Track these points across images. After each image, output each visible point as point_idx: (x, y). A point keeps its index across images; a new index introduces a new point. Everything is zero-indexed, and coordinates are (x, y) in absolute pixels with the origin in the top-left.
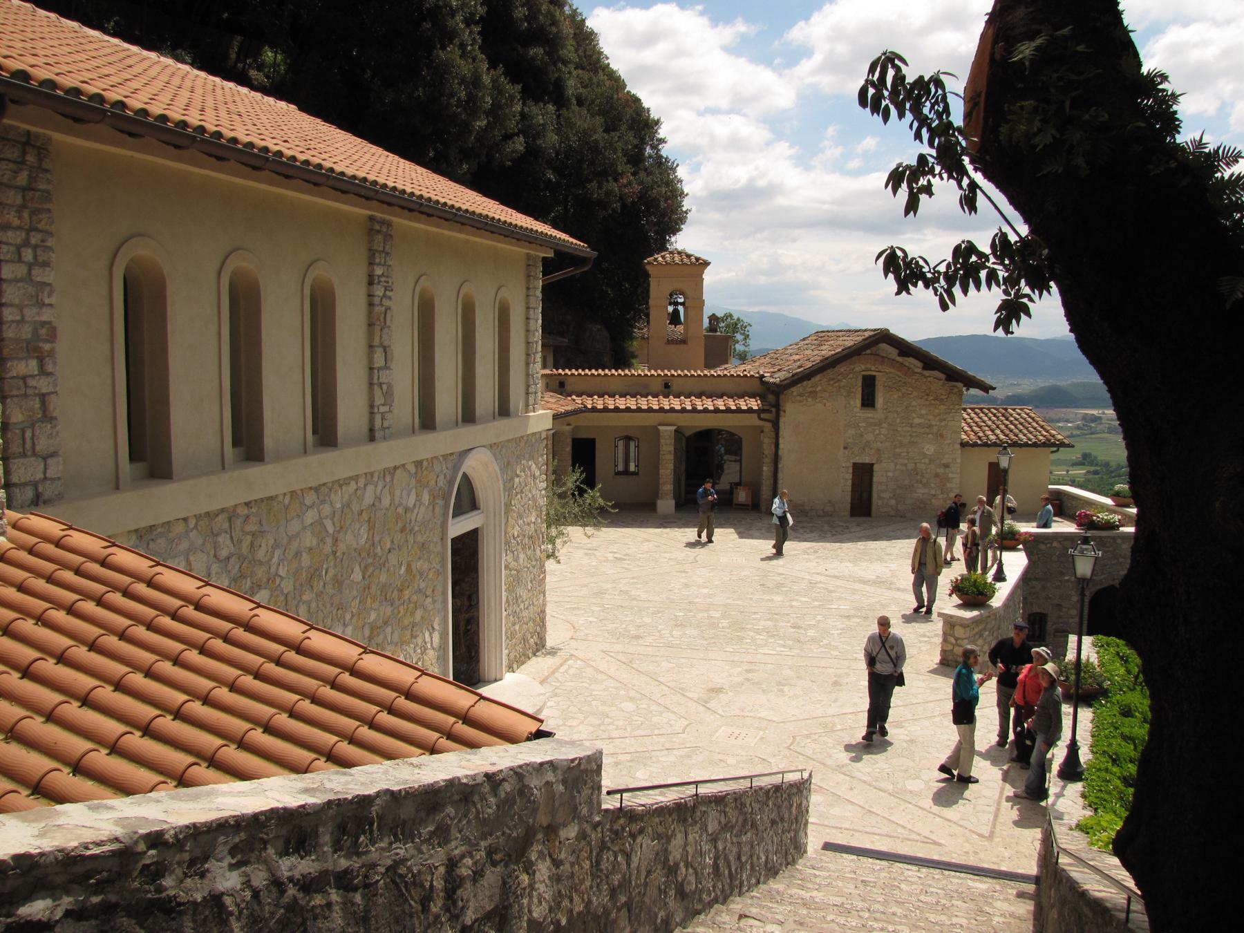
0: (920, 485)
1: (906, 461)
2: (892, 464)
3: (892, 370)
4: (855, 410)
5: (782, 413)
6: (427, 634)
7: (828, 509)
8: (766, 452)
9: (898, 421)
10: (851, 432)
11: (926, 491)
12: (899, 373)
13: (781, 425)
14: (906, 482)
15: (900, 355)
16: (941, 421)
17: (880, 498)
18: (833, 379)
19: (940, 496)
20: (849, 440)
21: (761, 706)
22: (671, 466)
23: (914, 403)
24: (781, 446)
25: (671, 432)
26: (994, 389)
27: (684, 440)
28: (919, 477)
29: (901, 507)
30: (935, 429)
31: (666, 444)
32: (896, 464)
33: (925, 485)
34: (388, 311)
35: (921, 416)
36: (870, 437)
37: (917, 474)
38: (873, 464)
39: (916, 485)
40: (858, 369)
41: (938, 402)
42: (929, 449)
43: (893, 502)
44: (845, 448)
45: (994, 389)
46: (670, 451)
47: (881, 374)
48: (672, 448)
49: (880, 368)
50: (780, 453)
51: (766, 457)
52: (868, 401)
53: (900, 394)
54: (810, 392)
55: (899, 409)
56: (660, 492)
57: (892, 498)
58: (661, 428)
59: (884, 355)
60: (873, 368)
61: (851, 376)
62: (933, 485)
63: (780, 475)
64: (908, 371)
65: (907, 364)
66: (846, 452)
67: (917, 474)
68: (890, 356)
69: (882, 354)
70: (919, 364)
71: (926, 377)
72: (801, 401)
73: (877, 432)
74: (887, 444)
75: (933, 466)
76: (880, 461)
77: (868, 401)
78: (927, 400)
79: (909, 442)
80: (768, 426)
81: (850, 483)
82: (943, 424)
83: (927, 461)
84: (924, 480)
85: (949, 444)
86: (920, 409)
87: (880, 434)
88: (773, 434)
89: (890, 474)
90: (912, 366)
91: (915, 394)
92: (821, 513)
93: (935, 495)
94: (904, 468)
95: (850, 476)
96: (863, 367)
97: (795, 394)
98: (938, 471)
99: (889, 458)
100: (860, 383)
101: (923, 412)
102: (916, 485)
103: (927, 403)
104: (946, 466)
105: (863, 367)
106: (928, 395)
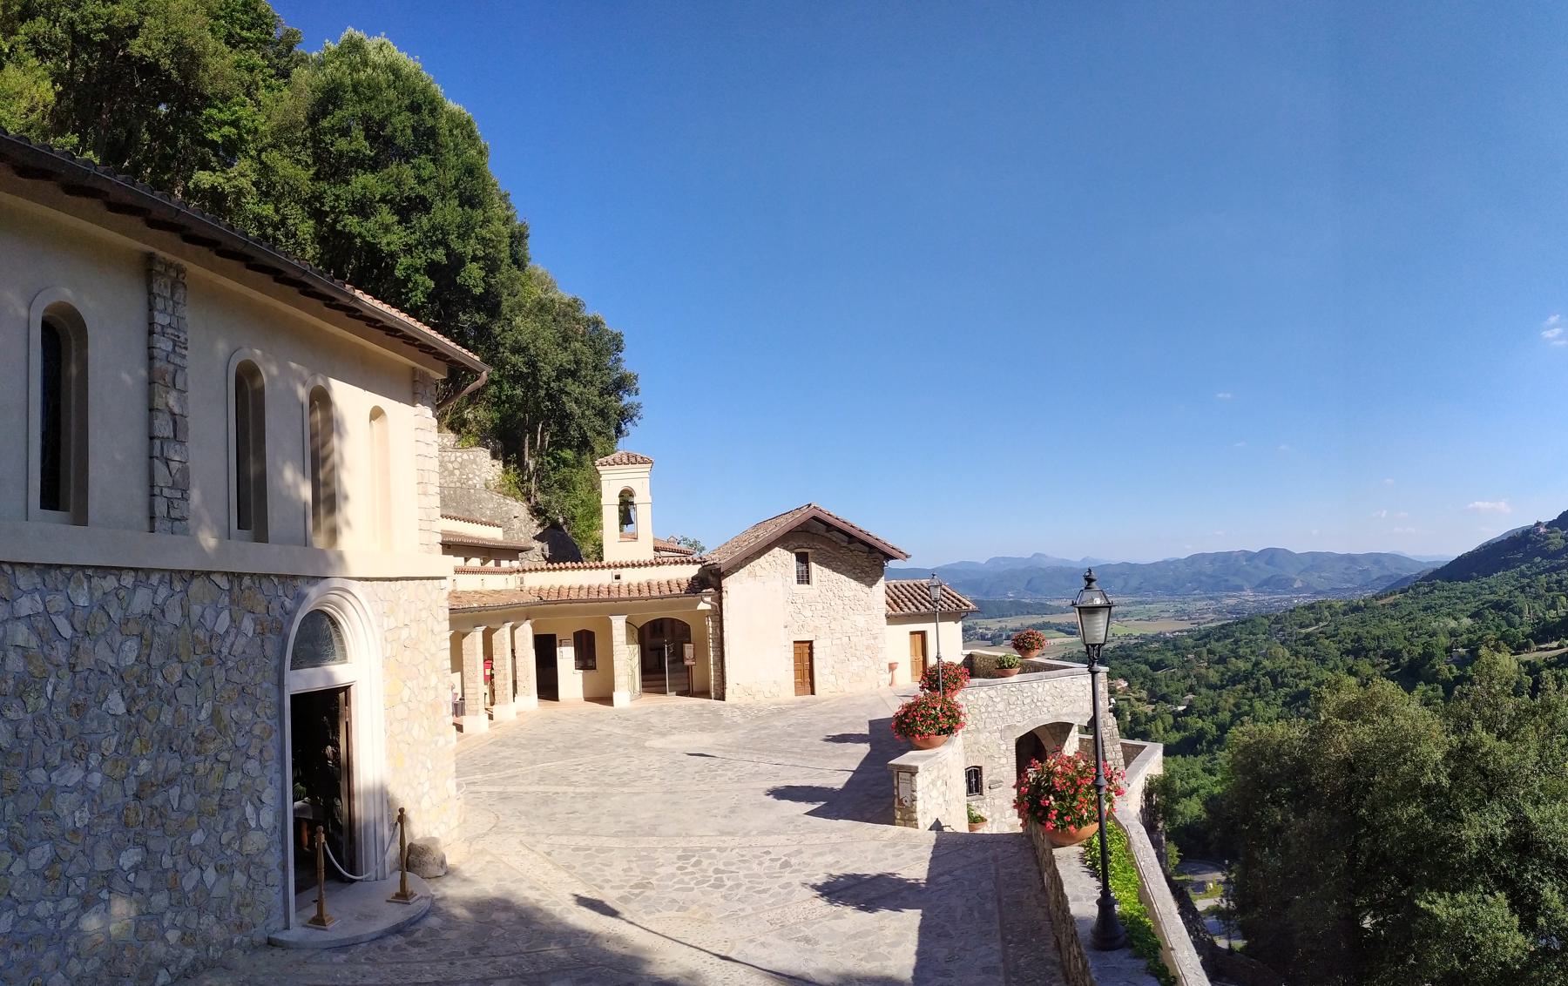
0: (855, 659)
5: (724, 594)
6: (249, 809)
10: (791, 608)
11: (860, 663)
19: (873, 667)
21: (693, 902)
28: (853, 650)
34: (179, 372)
37: (851, 647)
38: (811, 642)
39: (850, 658)
42: (861, 621)
43: (832, 678)
44: (786, 627)
50: (725, 635)
73: (813, 608)
83: (859, 633)
94: (838, 642)
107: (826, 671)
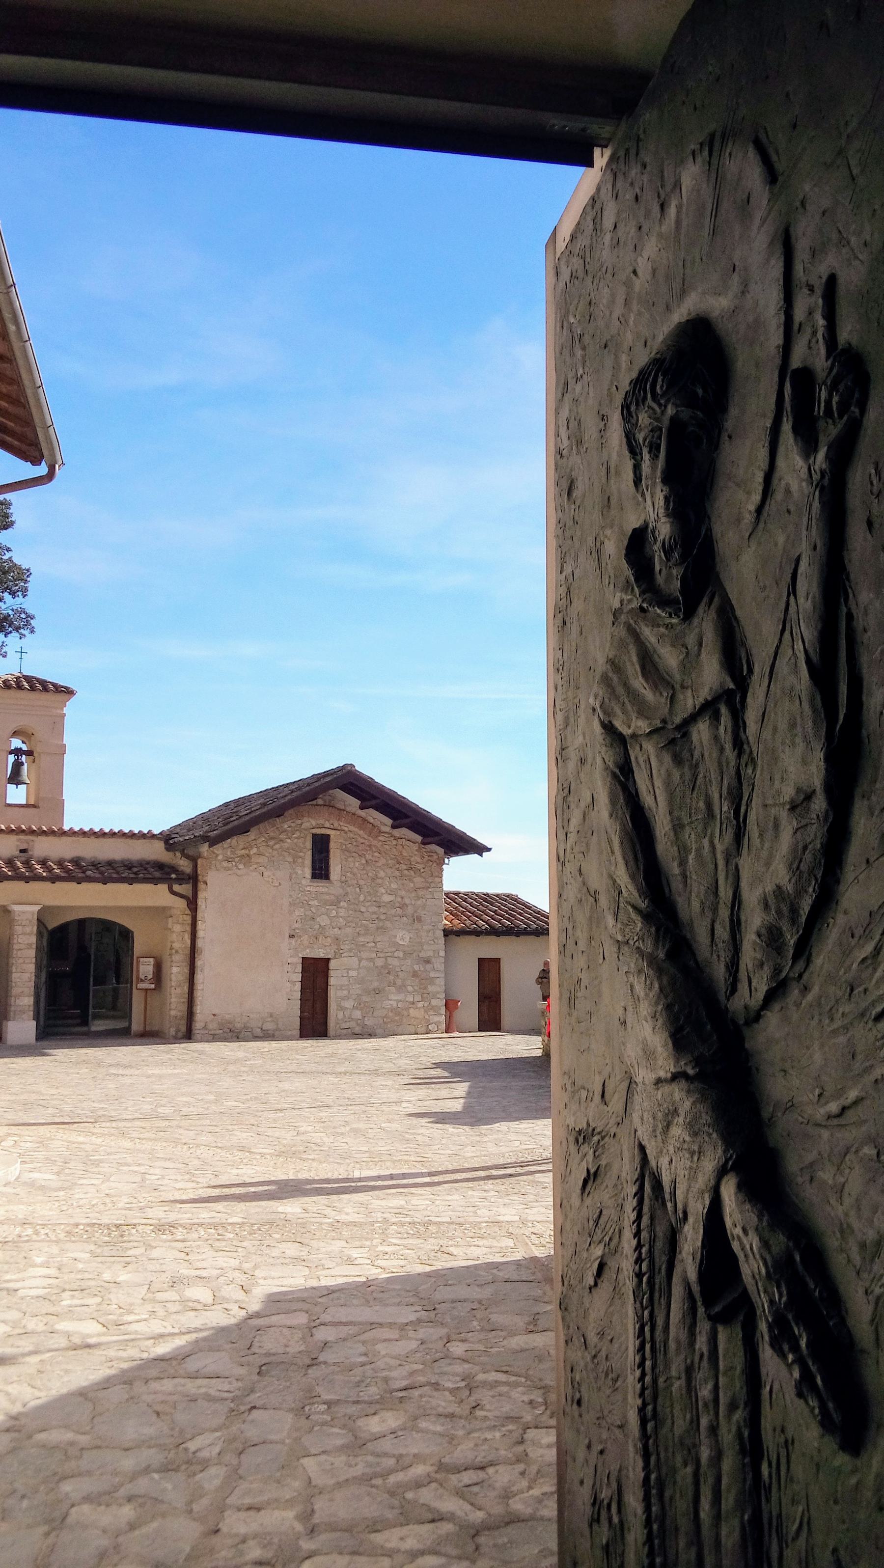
0: (392, 989)
1: (374, 955)
2: (355, 959)
3: (352, 828)
4: (304, 882)
7: (269, 1026)
8: (176, 945)
9: (362, 898)
12: (361, 832)
13: (201, 902)
14: (376, 984)
15: (362, 808)
16: (419, 898)
17: (342, 1009)
18: (272, 838)
19: (420, 1005)
20: (297, 925)
22: (32, 968)
23: (382, 874)
24: (200, 934)
25: (33, 914)
26: (489, 850)
27: (46, 935)
28: (391, 978)
29: (369, 1022)
30: (410, 910)
31: (24, 934)
32: (360, 961)
33: (401, 989)
35: (392, 893)
36: (324, 921)
37: (389, 973)
38: (327, 961)
40: (306, 825)
41: (412, 873)
42: (403, 937)
44: (292, 936)
45: (489, 850)
46: (30, 945)
47: (338, 833)
48: (33, 939)
49: (336, 825)
50: (200, 943)
51: (177, 952)
52: (321, 871)
53: (364, 862)
54: (242, 856)
55: (362, 882)
56: (13, 1009)
57: (357, 1008)
58: (16, 908)
59: (343, 808)
60: (327, 825)
61: (297, 834)
62: (410, 989)
63: (199, 977)
64: (374, 830)
65: (372, 821)
66: (293, 941)
67: (389, 973)
68: (348, 809)
69: (338, 805)
70: (389, 821)
71: (396, 839)
72: (227, 869)
73: (334, 913)
74: (348, 930)
75: (409, 962)
76: (338, 955)
77: (321, 871)
78: (398, 869)
79: (378, 928)
80: (181, 904)
81: (298, 986)
82: (419, 902)
83: (401, 954)
84: (399, 982)
85: (429, 931)
86: (390, 883)
87: (337, 917)
88: (188, 919)
89: (353, 973)
90: (377, 823)
91: (383, 861)
92: (261, 1035)
93: (413, 1003)
94: (371, 965)
95: (299, 977)
96: (314, 823)
97: (220, 857)
98: (416, 967)
99: (350, 950)
100: (309, 844)
101: (394, 886)
102: (387, 988)
103: (397, 873)
104: (428, 961)
105: (314, 823)
106: (399, 863)
107: (349, 1004)
